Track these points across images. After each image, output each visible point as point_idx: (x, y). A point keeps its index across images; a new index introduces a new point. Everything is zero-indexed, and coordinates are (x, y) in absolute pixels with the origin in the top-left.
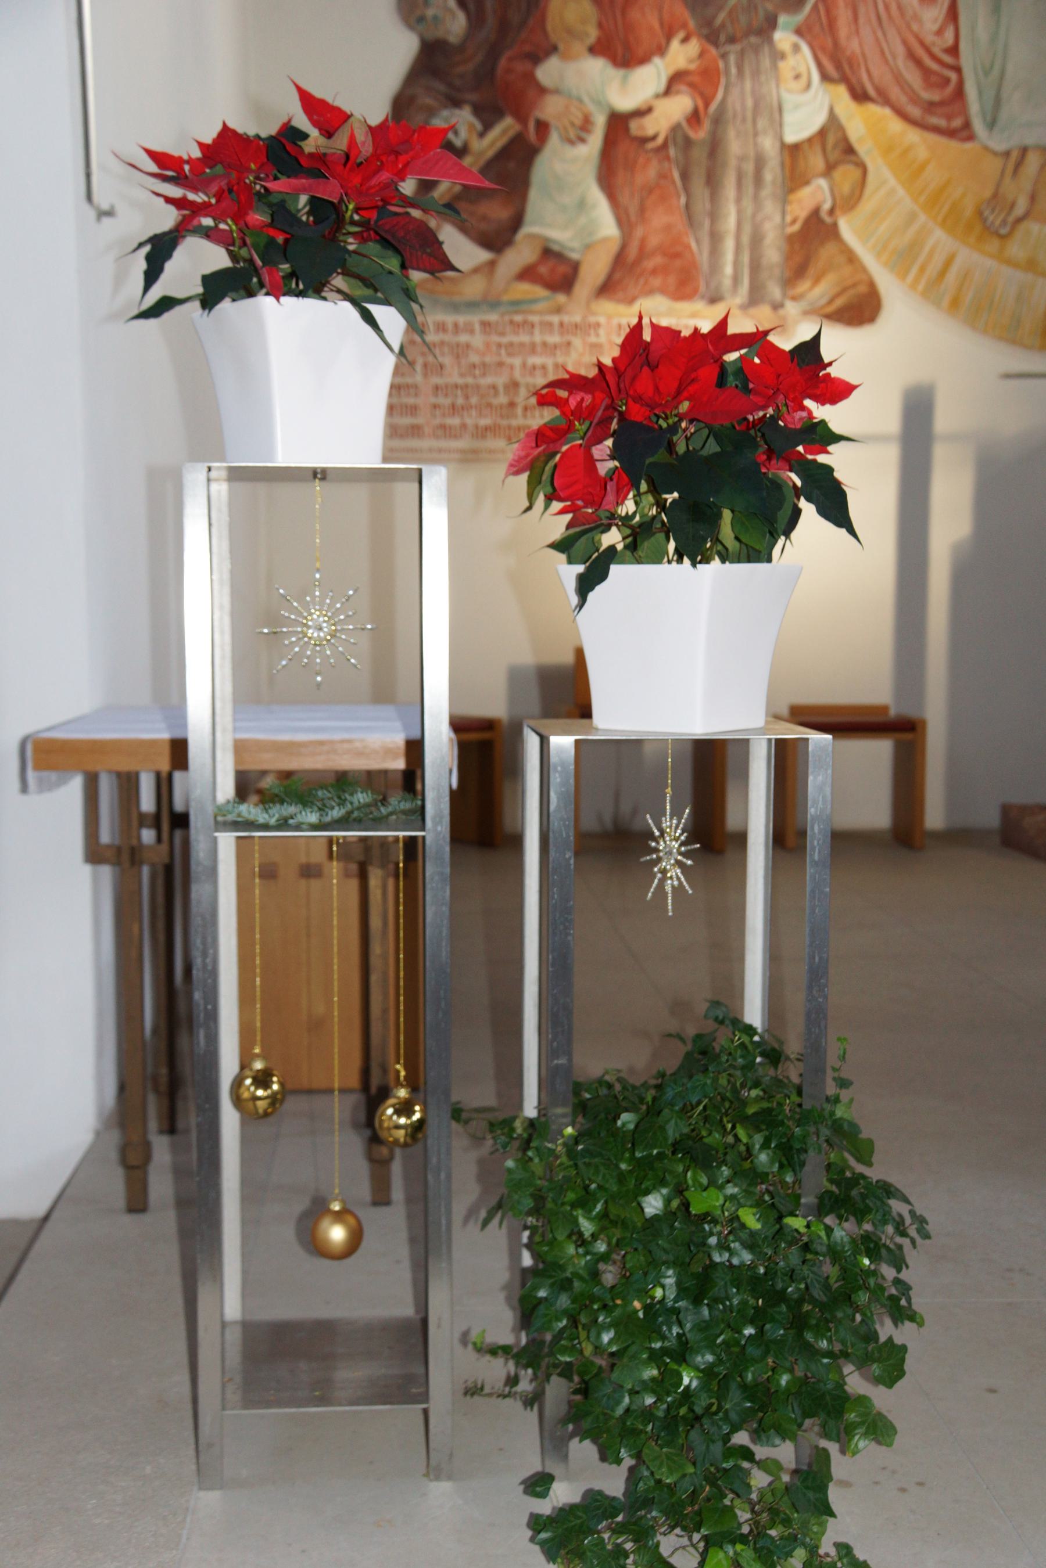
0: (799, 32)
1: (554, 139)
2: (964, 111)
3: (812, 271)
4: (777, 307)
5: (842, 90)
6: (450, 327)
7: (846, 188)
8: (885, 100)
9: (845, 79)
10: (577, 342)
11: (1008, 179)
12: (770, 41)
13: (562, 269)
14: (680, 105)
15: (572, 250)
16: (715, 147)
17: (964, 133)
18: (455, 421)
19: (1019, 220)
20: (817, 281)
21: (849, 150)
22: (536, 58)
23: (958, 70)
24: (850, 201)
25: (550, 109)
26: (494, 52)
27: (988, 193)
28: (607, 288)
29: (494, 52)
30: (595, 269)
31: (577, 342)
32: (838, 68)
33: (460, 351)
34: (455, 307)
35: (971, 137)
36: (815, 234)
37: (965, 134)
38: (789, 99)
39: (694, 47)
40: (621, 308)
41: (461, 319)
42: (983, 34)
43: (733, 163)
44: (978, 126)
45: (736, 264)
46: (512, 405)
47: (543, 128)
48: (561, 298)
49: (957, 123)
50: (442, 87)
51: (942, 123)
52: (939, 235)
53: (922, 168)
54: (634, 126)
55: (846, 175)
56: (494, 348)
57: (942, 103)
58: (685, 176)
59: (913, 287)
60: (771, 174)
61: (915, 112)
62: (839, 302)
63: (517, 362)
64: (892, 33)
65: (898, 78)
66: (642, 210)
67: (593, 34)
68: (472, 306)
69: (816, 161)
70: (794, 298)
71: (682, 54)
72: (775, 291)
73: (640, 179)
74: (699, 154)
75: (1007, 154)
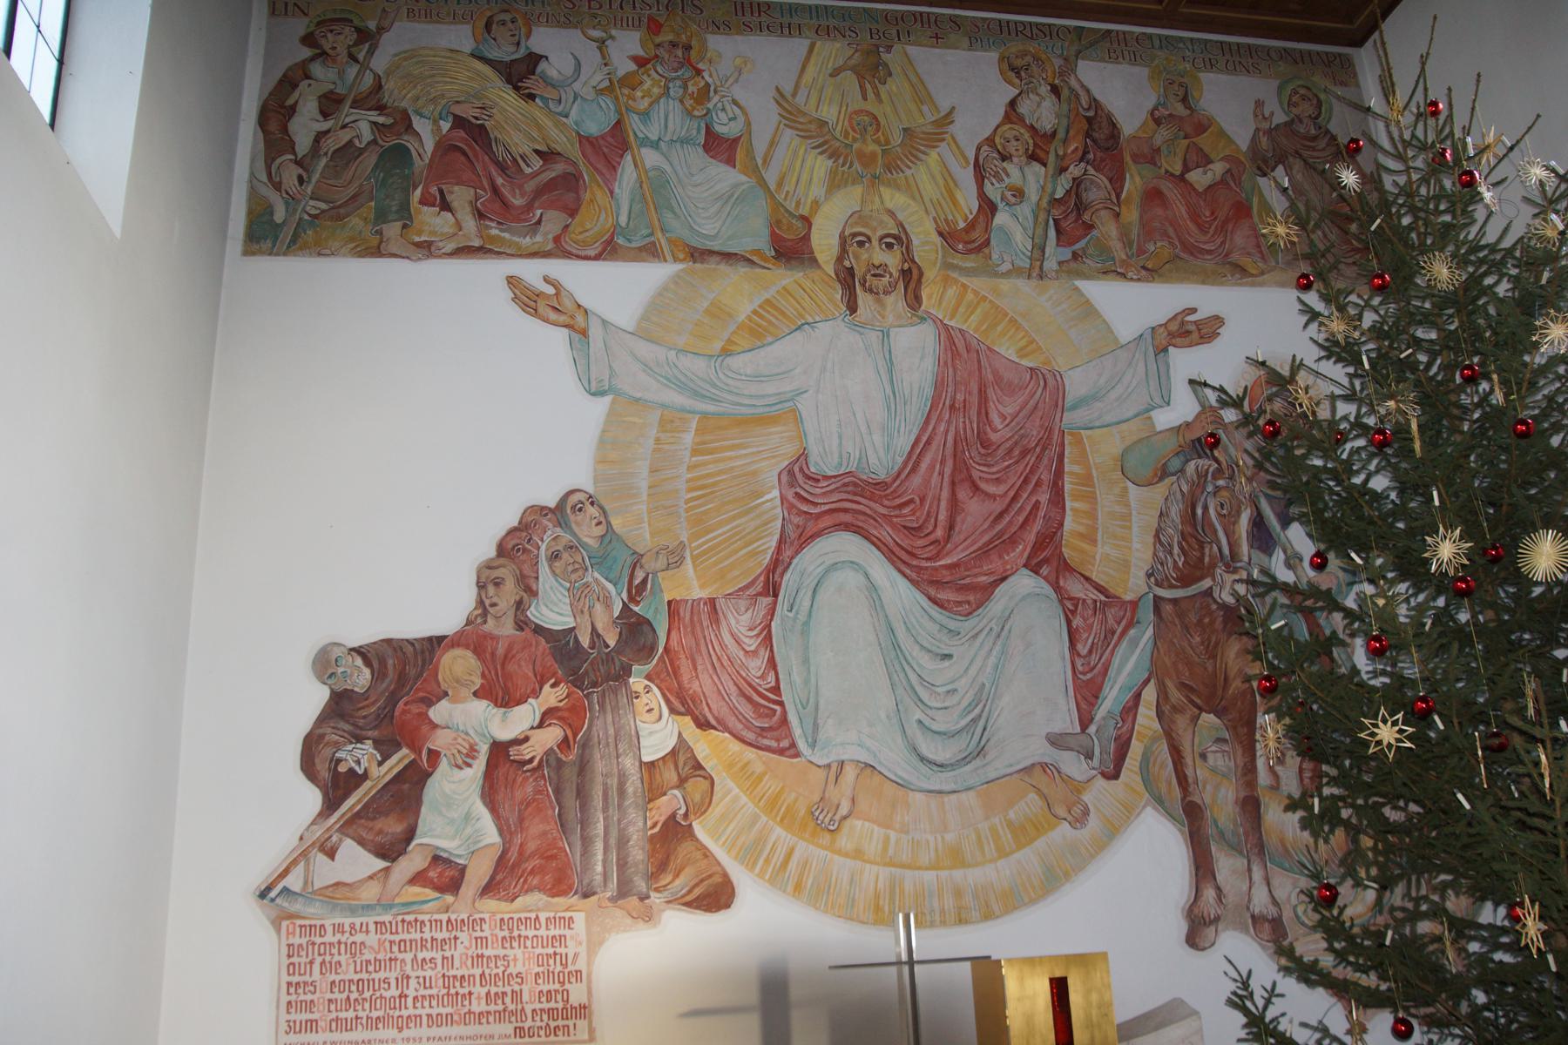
0: (648, 677)
1: (444, 764)
2: (790, 735)
3: (672, 866)
4: (644, 898)
5: (688, 719)
6: (347, 928)
7: (697, 798)
9: (689, 712)
10: (464, 936)
11: (831, 786)
12: (626, 684)
13: (450, 873)
14: (552, 736)
15: (460, 856)
16: (583, 766)
17: (791, 751)
18: (351, 1014)
19: (845, 818)
20: (677, 876)
22: (430, 702)
23: (781, 704)
24: (703, 807)
25: (439, 741)
26: (393, 699)
27: (816, 798)
28: (489, 889)
29: (393, 699)
30: (479, 872)
31: (464, 936)
32: (683, 703)
33: (355, 949)
34: (353, 911)
35: (797, 755)
36: (674, 832)
37: (792, 752)
38: (644, 729)
39: (562, 690)
40: (503, 905)
41: (357, 921)
42: (797, 678)
43: (599, 779)
44: (802, 745)
45: (605, 861)
46: (403, 996)
47: (434, 756)
48: (449, 898)
49: (785, 743)
50: (347, 727)
51: (774, 744)
52: (779, 831)
53: (760, 778)
54: (513, 751)
55: (697, 787)
56: (387, 944)
57: (771, 729)
58: (558, 792)
59: (761, 875)
60: (634, 785)
61: (750, 736)
62: (697, 892)
63: (409, 957)
64: (725, 677)
65: (733, 710)
66: (521, 820)
67: (478, 682)
68: (368, 908)
69: (670, 775)
70: (657, 890)
71: (552, 696)
72: (641, 884)
73: (519, 795)
74: (570, 774)
75: (829, 766)
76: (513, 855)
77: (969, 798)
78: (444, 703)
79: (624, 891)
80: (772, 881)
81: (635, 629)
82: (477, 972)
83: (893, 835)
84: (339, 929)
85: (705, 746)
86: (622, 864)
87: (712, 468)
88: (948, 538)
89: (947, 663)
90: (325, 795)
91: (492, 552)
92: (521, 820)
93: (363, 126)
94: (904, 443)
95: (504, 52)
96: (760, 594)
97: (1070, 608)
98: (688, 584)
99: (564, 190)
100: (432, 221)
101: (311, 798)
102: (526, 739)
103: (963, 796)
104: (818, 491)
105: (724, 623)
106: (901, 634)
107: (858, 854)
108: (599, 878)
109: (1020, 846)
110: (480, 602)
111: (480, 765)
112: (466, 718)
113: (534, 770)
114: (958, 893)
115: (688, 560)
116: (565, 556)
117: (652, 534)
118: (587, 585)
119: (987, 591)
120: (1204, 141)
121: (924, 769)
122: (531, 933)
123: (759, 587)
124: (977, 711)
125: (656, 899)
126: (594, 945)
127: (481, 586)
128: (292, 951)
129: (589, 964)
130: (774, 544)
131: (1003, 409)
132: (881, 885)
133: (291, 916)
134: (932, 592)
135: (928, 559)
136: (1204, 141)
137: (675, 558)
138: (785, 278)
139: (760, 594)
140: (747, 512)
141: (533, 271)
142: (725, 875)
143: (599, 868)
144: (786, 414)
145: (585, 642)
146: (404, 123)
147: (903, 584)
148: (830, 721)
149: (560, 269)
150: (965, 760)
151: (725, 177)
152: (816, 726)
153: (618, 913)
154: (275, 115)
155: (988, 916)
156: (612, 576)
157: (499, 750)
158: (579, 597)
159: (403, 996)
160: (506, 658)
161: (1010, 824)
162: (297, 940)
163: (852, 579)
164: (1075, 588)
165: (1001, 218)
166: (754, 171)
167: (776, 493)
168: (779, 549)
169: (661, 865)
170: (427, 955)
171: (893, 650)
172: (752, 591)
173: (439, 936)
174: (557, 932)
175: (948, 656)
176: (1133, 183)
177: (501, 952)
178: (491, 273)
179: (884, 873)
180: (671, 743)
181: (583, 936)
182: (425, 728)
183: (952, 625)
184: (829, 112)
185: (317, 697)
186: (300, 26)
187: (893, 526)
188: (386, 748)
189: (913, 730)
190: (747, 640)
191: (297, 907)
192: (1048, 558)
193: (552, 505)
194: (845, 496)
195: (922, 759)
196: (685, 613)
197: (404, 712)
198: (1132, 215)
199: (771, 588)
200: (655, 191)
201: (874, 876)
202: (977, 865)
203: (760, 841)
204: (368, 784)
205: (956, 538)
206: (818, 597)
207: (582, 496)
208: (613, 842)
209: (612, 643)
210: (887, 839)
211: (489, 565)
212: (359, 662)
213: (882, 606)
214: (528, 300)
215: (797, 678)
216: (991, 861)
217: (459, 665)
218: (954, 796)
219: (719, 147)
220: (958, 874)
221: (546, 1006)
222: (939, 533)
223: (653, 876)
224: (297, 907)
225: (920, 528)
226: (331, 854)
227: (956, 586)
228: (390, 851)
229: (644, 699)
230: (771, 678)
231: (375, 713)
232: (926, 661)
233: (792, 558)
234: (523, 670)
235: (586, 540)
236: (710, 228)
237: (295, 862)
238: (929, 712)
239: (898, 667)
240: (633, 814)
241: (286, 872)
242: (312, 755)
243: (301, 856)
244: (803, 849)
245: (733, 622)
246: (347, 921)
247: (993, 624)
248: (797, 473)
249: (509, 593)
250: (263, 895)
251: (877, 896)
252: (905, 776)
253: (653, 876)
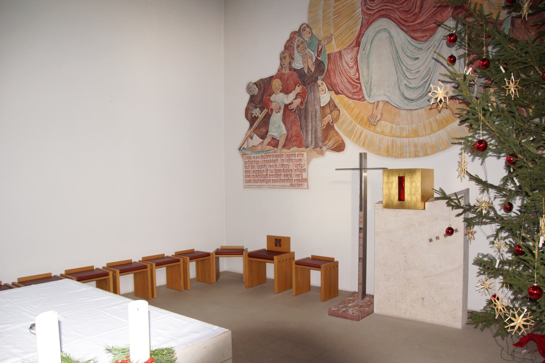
0: (323, 80)
2: (362, 94)
3: (328, 138)
4: (321, 148)
5: (333, 92)
7: (335, 117)
8: (344, 94)
9: (333, 90)
11: (375, 110)
12: (317, 83)
14: (299, 101)
16: (306, 110)
17: (363, 99)
18: (257, 179)
19: (379, 121)
20: (330, 141)
21: (336, 107)
22: (270, 95)
23: (360, 83)
24: (336, 120)
25: (273, 106)
27: (370, 115)
28: (284, 146)
30: (282, 142)
32: (332, 87)
34: (256, 153)
35: (364, 100)
36: (329, 127)
37: (363, 99)
39: (301, 87)
40: (287, 151)
41: (257, 155)
42: (365, 74)
43: (310, 113)
45: (311, 137)
46: (267, 175)
47: (272, 110)
48: (276, 149)
49: (361, 97)
50: (254, 105)
51: (357, 97)
52: (358, 126)
53: (353, 109)
55: (335, 113)
57: (357, 92)
58: (300, 117)
59: (353, 141)
60: (319, 114)
61: (350, 95)
62: (335, 146)
63: (268, 164)
64: (343, 77)
65: (346, 87)
66: (291, 126)
68: (259, 152)
69: (328, 110)
70: (324, 145)
71: (298, 89)
73: (291, 119)
74: (303, 112)
75: (374, 103)
76: (289, 137)
77: (422, 111)
78: (274, 95)
79: (316, 146)
80: (356, 142)
81: (319, 64)
82: (282, 169)
83: (394, 126)
84: (254, 157)
85: (337, 99)
86: (316, 138)
87: (341, 6)
88: (420, 12)
89: (417, 61)
90: (250, 123)
91: (283, 49)
92: (291, 126)
96: (354, 47)
98: (333, 48)
101: (247, 124)
102: (292, 103)
103: (420, 111)
104: (374, 5)
105: (343, 59)
106: (400, 52)
107: (382, 133)
108: (310, 142)
109: (440, 129)
110: (281, 64)
111: (282, 111)
112: (280, 99)
113: (294, 112)
114: (415, 146)
115: (334, 40)
116: (301, 46)
117: (324, 33)
118: (306, 54)
121: (406, 101)
122: (294, 158)
123: (354, 44)
124: (427, 78)
125: (324, 148)
126: (309, 161)
127: (281, 60)
128: (246, 163)
129: (307, 167)
130: (359, 28)
132: (389, 143)
133: (245, 154)
134: (412, 34)
135: (412, 22)
137: (329, 39)
139: (354, 47)
140: (351, 18)
142: (343, 141)
143: (310, 139)
145: (306, 72)
147: (402, 33)
148: (375, 88)
150: (421, 98)
152: (371, 90)
153: (315, 152)
155: (426, 154)
156: (313, 49)
157: (286, 106)
158: (305, 57)
159: (267, 175)
160: (287, 80)
161: (436, 120)
162: (246, 160)
163: (384, 35)
167: (360, 9)
168: (361, 29)
169: (325, 138)
170: (271, 164)
172: (352, 46)
173: (274, 159)
174: (299, 158)
175: (418, 58)
177: (287, 163)
179: (390, 139)
180: (328, 100)
181: (306, 159)
182: (270, 103)
183: (420, 46)
185: (247, 97)
187: (400, 12)
188: (262, 109)
189: (403, 88)
190: (350, 63)
191: (246, 152)
193: (297, 30)
194: (383, 4)
195: (406, 98)
196: (332, 57)
197: (265, 99)
201: (387, 140)
202: (423, 136)
203: (353, 129)
204: (258, 119)
205: (423, 11)
206: (373, 44)
207: (304, 26)
208: (313, 131)
209: (313, 71)
210: (392, 127)
211: (283, 53)
212: (255, 86)
213: (394, 43)
215: (365, 74)
216: (428, 135)
217: (277, 84)
218: (416, 111)
220: (416, 139)
221: (297, 178)
222: (417, 10)
223: (323, 141)
224: (246, 152)
225: (409, 10)
226: (252, 138)
228: (263, 137)
229: (321, 87)
230: (357, 75)
232: (409, 62)
233: (365, 32)
234: (291, 82)
235: (306, 39)
237: (245, 141)
238: (409, 81)
239: (399, 65)
240: (319, 123)
241: (243, 144)
243: (246, 140)
244: (366, 131)
245: (346, 57)
246: (255, 155)
247: (435, 43)
249: (288, 59)
250: (240, 149)
251: (388, 147)
252: (398, 104)
253: (323, 141)
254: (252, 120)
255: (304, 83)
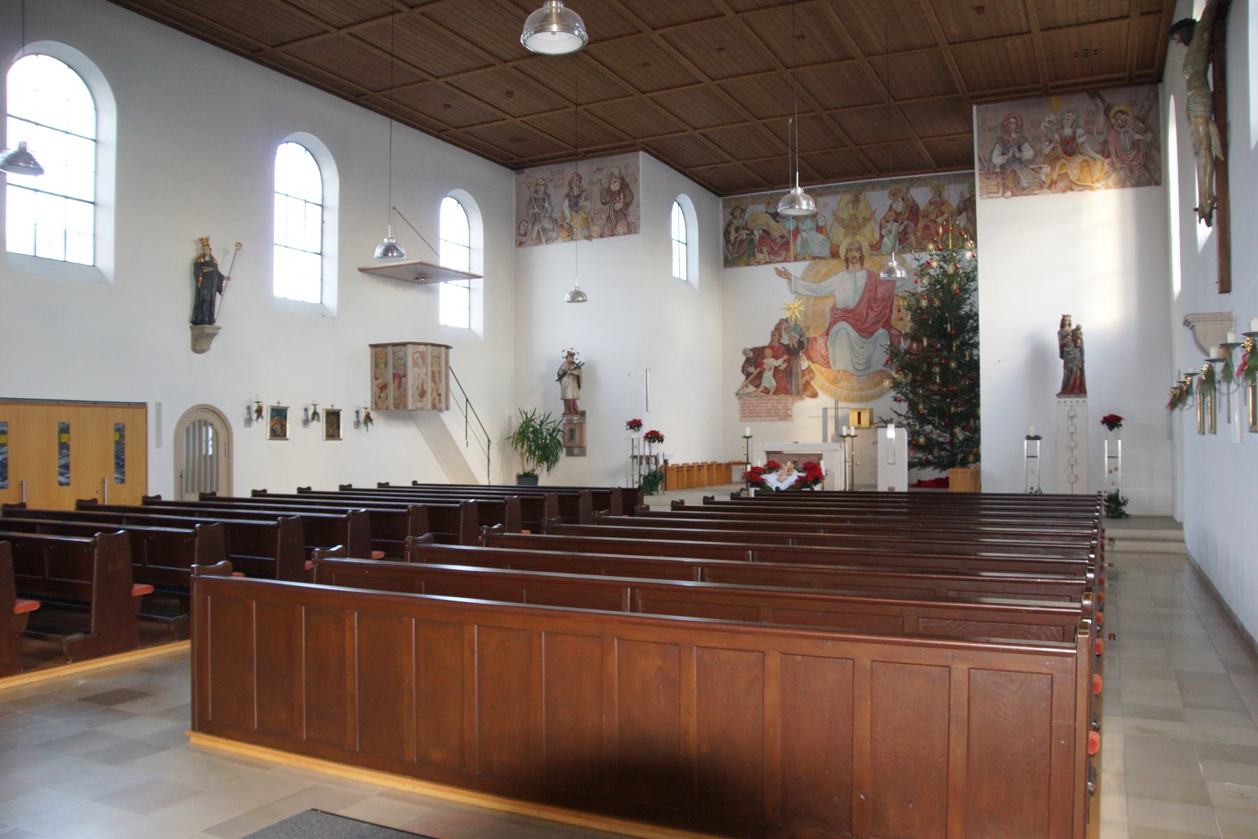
14: (785, 365)
24: (812, 378)
28: (775, 393)
30: (772, 391)
32: (809, 358)
36: (807, 383)
71: (785, 357)
81: (801, 344)
85: (813, 367)
93: (744, 234)
94: (857, 300)
95: (772, 211)
97: (891, 336)
99: (786, 245)
100: (760, 256)
101: (743, 377)
112: (770, 362)
119: (872, 333)
120: (943, 208)
126: (793, 403)
131: (881, 289)
136: (943, 208)
137: (808, 328)
138: (834, 262)
141: (780, 266)
144: (831, 295)
146: (752, 233)
149: (785, 265)
151: (820, 237)
154: (727, 233)
157: (776, 368)
158: (790, 338)
164: (893, 332)
165: (885, 239)
166: (827, 235)
171: (852, 347)
176: (921, 224)
178: (771, 267)
184: (845, 216)
185: (744, 359)
186: (729, 210)
192: (888, 325)
198: (919, 234)
199: (827, 334)
200: (805, 243)
214: (780, 273)
217: (768, 352)
219: (819, 229)
227: (866, 332)
228: (757, 386)
231: (754, 359)
236: (817, 251)
242: (744, 370)
248: (834, 309)
254: (748, 375)
255: (789, 354)
